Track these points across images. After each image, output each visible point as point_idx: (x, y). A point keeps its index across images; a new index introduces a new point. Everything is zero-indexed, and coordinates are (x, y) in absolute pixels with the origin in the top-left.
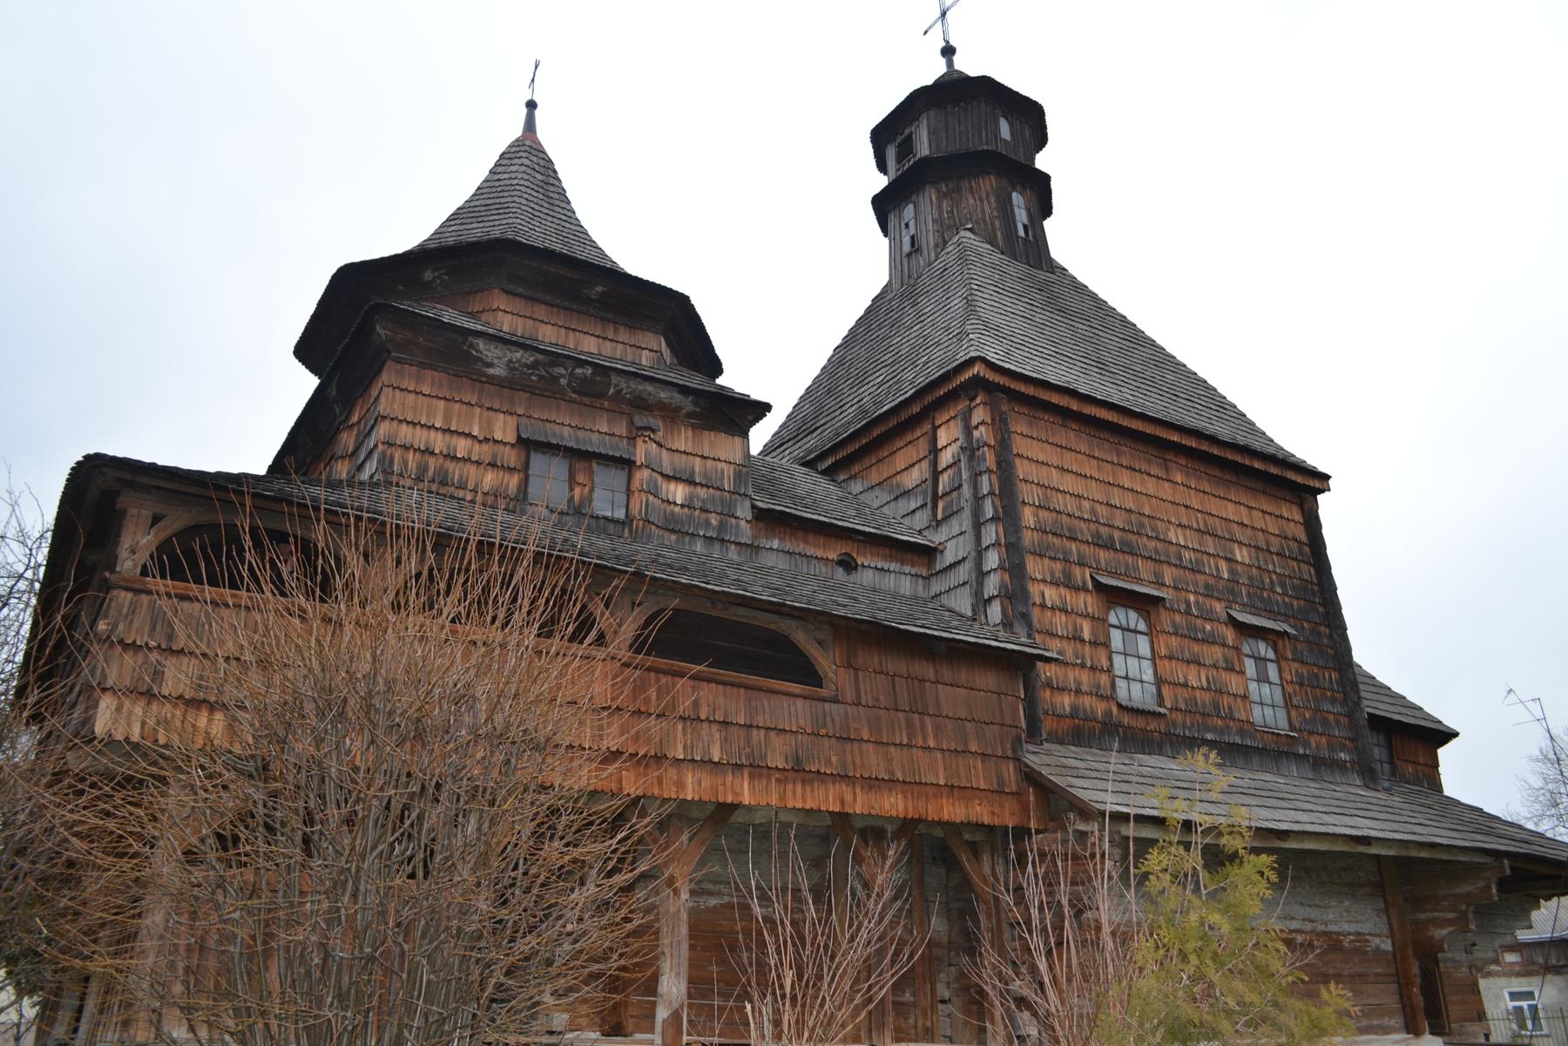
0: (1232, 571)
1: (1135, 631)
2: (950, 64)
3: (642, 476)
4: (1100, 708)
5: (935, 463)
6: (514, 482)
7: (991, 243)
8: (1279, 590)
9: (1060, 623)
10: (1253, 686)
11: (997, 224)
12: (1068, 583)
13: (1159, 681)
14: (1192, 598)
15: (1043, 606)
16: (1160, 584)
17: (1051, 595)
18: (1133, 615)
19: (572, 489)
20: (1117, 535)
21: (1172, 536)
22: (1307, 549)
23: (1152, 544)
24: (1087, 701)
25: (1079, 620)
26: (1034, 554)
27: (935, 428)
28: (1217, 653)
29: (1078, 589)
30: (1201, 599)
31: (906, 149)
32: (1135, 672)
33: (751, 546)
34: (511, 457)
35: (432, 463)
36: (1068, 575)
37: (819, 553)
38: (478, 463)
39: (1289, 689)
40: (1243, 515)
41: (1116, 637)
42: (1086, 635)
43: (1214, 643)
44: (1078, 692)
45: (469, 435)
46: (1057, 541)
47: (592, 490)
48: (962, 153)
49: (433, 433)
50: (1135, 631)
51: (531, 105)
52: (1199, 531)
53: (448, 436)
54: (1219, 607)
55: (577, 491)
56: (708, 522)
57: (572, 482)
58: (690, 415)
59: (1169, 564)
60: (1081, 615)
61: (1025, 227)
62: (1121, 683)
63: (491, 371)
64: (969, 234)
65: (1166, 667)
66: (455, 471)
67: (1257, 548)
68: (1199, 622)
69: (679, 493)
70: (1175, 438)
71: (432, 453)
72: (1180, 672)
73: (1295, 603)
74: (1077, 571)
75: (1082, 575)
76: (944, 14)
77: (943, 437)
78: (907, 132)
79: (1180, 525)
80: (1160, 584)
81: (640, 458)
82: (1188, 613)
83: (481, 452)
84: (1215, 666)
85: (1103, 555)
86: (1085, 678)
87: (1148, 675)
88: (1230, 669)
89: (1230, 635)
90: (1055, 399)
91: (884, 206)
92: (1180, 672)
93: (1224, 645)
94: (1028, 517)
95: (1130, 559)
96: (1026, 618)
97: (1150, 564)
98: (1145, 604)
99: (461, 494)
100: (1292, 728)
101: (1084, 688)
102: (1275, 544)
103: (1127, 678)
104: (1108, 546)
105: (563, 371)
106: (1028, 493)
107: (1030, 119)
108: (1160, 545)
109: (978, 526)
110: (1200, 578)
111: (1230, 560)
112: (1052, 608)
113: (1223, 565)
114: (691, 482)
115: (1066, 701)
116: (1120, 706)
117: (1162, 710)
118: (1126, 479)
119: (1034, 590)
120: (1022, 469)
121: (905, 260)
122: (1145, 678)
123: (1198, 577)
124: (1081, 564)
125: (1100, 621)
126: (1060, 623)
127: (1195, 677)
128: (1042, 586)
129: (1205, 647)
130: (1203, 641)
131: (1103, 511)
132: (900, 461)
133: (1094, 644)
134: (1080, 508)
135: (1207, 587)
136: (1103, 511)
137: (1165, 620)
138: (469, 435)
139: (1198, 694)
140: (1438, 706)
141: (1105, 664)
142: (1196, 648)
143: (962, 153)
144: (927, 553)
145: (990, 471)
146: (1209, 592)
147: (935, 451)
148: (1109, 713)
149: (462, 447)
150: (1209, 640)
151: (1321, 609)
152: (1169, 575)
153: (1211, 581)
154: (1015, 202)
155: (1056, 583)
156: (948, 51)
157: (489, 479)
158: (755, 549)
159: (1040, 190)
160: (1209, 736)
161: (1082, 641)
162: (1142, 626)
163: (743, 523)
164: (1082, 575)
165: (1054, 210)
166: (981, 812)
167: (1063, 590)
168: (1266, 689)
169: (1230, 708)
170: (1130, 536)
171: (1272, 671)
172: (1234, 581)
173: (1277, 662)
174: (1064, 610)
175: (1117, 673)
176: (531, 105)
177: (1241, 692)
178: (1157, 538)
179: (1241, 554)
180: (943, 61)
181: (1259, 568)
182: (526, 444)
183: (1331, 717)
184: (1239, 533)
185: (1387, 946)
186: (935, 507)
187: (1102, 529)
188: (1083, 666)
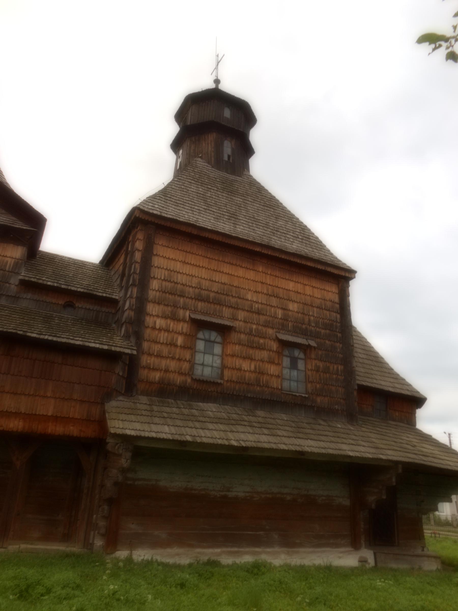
1: (214, 342)
4: (179, 379)
7: (208, 163)
10: (286, 372)
11: (213, 154)
12: (174, 318)
13: (223, 367)
14: (254, 327)
15: (154, 328)
17: (160, 323)
20: (212, 295)
21: (249, 297)
22: (338, 306)
23: (233, 300)
24: (171, 376)
25: (176, 336)
26: (154, 302)
28: (265, 354)
29: (179, 320)
30: (260, 328)
32: (208, 361)
33: (15, 297)
37: (54, 301)
39: (309, 373)
40: (299, 288)
41: (200, 345)
43: (263, 349)
50: (214, 342)
52: (267, 294)
54: (270, 331)
59: (243, 310)
60: (179, 333)
61: (229, 157)
62: (196, 367)
64: (199, 159)
65: (230, 361)
68: (256, 339)
70: (258, 249)
72: (238, 362)
73: (323, 331)
80: (234, 319)
85: (200, 305)
86: (173, 365)
88: (271, 362)
90: (183, 228)
92: (238, 362)
93: (270, 350)
94: (155, 284)
95: (218, 307)
97: (231, 310)
98: (224, 330)
102: (318, 302)
103: (203, 365)
104: (206, 300)
106: (155, 272)
108: (239, 301)
110: (262, 318)
112: (160, 330)
115: (157, 376)
117: (222, 382)
118: (226, 268)
119: (149, 321)
120: (156, 261)
122: (215, 365)
123: (261, 317)
124: (185, 308)
126: (163, 337)
127: (246, 365)
128: (155, 318)
129: (257, 352)
130: (257, 348)
133: (184, 347)
137: (234, 336)
139: (247, 374)
140: (419, 383)
141: (188, 357)
142: (251, 351)
144: (113, 302)
145: (137, 262)
146: (266, 325)
150: (261, 348)
151: (339, 335)
152: (241, 315)
155: (165, 317)
158: (16, 298)
160: (249, 396)
161: (176, 346)
162: (219, 339)
163: (13, 286)
165: (255, 150)
166: (73, 430)
167: (169, 321)
168: (295, 373)
170: (221, 296)
172: (285, 318)
173: (305, 360)
174: (167, 330)
175: (197, 362)
179: (293, 307)
184: (293, 296)
185: (347, 502)
188: (173, 358)
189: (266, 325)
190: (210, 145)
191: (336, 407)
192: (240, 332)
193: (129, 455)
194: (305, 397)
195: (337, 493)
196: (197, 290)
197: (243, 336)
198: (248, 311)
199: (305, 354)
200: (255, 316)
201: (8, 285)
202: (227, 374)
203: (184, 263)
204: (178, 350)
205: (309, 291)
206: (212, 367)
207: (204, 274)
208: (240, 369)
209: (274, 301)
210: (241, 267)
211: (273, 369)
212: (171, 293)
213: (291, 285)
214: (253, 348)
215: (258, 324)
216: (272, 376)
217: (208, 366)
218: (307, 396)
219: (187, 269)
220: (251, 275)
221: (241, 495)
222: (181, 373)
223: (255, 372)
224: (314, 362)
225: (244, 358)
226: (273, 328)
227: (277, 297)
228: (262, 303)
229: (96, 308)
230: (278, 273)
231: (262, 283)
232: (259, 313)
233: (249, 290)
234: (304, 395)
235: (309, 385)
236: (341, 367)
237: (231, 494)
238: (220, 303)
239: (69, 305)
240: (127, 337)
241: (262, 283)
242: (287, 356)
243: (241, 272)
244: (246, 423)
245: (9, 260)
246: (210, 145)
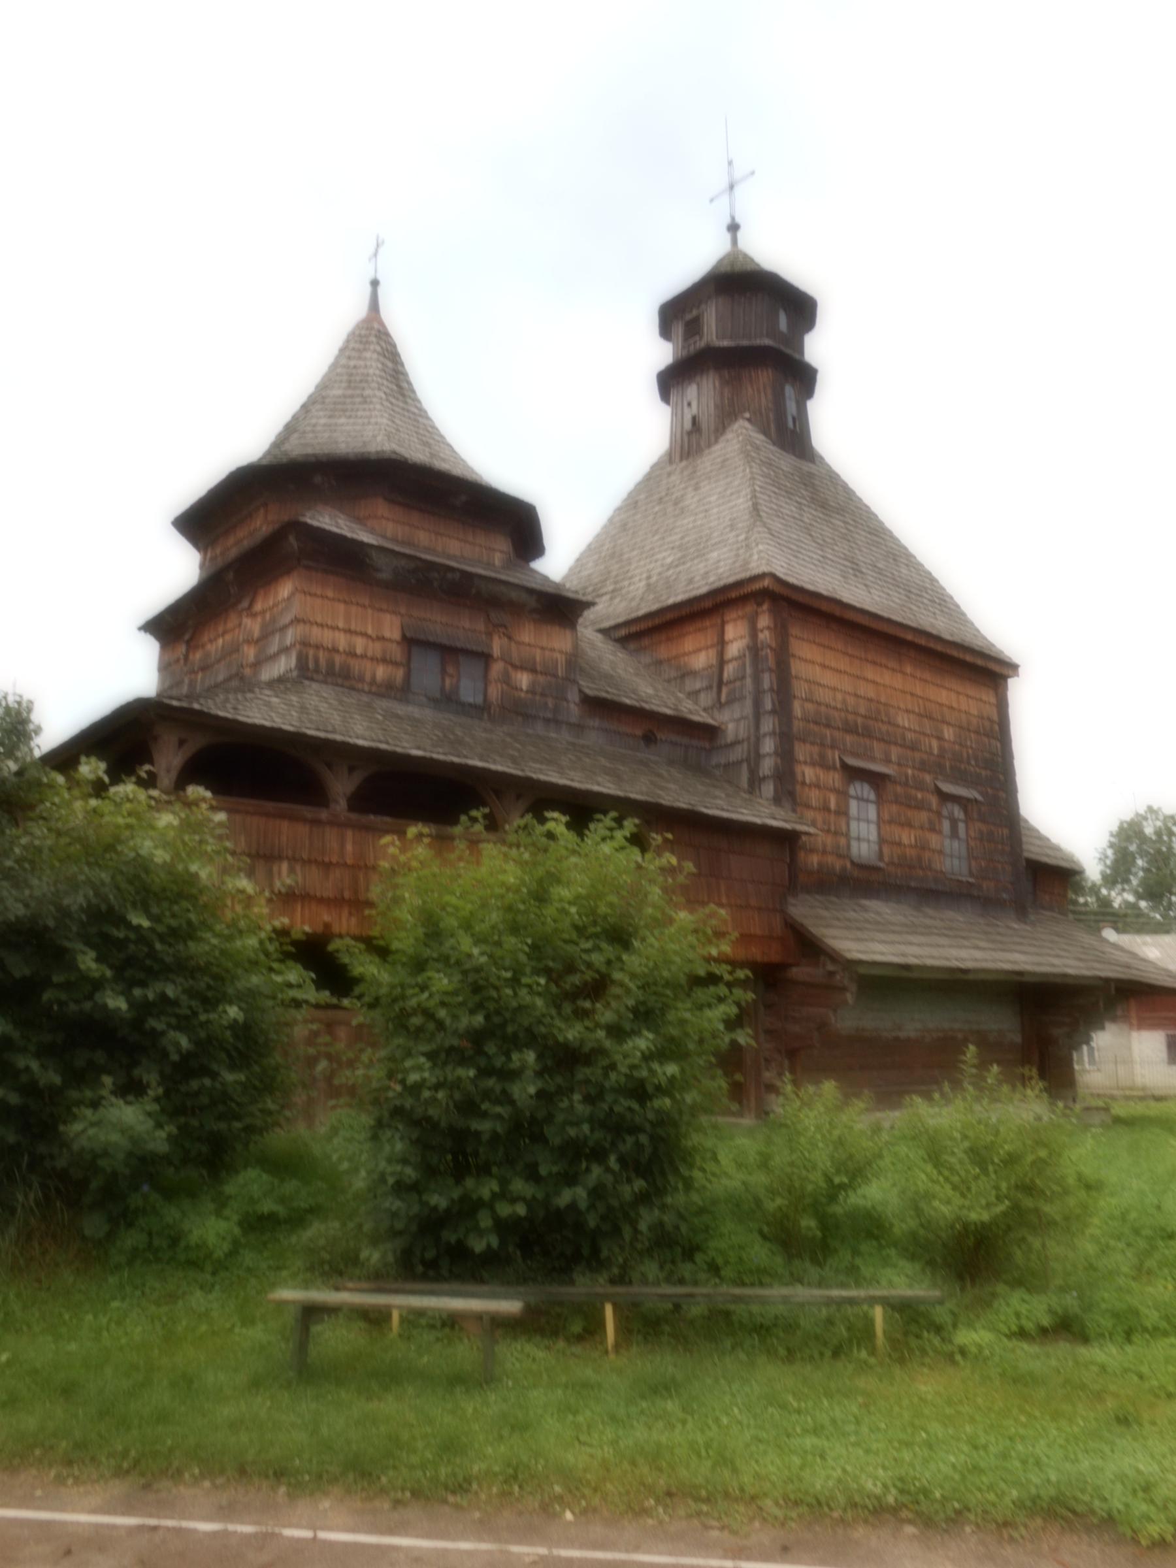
0: (941, 748)
2: (734, 241)
3: (497, 668)
4: (838, 864)
5: (721, 654)
6: (400, 674)
8: (973, 762)
9: (814, 796)
10: (947, 842)
11: (771, 416)
12: (822, 763)
13: (882, 841)
14: (910, 772)
15: (803, 783)
16: (888, 761)
18: (866, 787)
20: (860, 720)
21: (903, 720)
23: (884, 728)
24: (830, 859)
28: (924, 816)
30: (916, 772)
31: (693, 328)
32: (864, 831)
34: (397, 652)
35: (338, 659)
36: (822, 756)
38: (372, 659)
39: (972, 843)
41: (853, 805)
42: (833, 806)
44: (824, 852)
45: (364, 635)
46: (816, 728)
47: (458, 681)
48: (741, 341)
49: (337, 634)
50: (867, 801)
51: (375, 284)
52: (920, 715)
53: (348, 636)
54: (928, 778)
55: (448, 681)
56: (546, 704)
57: (444, 672)
62: (854, 844)
66: (356, 665)
67: (961, 727)
68: (913, 792)
69: (524, 680)
70: (909, 637)
71: (337, 651)
73: (983, 773)
74: (829, 753)
75: (834, 756)
76: (731, 187)
77: (731, 631)
78: (695, 312)
79: (907, 711)
81: (496, 651)
82: (906, 784)
83: (376, 649)
84: (922, 828)
85: (849, 739)
87: (873, 836)
88: (932, 829)
89: (934, 801)
90: (824, 607)
91: (670, 381)
93: (930, 810)
94: (797, 709)
96: (792, 795)
98: (876, 780)
100: (971, 874)
101: (829, 849)
105: (436, 575)
106: (800, 689)
107: (799, 308)
109: (757, 716)
110: (917, 755)
111: (940, 738)
114: (533, 670)
116: (852, 863)
117: (882, 865)
118: (870, 673)
120: (797, 667)
121: (689, 444)
125: (843, 795)
131: (851, 701)
132: (689, 643)
134: (834, 699)
136: (851, 701)
138: (364, 635)
142: (910, 813)
143: (741, 341)
144: (709, 732)
146: (923, 767)
147: (722, 643)
148: (844, 869)
149: (360, 644)
150: (920, 806)
152: (895, 753)
153: (925, 757)
154: (787, 394)
156: (734, 228)
157: (381, 672)
159: (803, 378)
160: (913, 884)
162: (872, 796)
163: (572, 706)
164: (834, 756)
168: (956, 844)
169: (929, 860)
171: (961, 826)
172: (941, 755)
173: (966, 822)
174: (818, 786)
176: (375, 284)
177: (938, 848)
178: (889, 723)
179: (948, 733)
180: (728, 237)
181: (961, 745)
182: (412, 642)
183: (1000, 866)
185: (1017, 1038)
189: (923, 767)
190: (762, 394)
191: (1005, 896)
192: (895, 782)
193: (854, 988)
194: (968, 882)
195: (1003, 1023)
196: (843, 714)
197: (899, 789)
198: (901, 746)
199: (966, 812)
200: (909, 753)
201: (565, 704)
202: (886, 850)
203: (824, 666)
204: (832, 818)
205: (964, 704)
206: (869, 841)
207: (846, 684)
208: (899, 844)
209: (928, 726)
210: (887, 667)
211: (934, 840)
212: (816, 723)
213: (944, 696)
214: (909, 806)
215: (914, 767)
216: (934, 851)
217: (864, 840)
218: (971, 880)
219: (829, 679)
220: (897, 681)
221: (913, 1035)
222: (840, 856)
223: (916, 846)
224: (978, 825)
225: (902, 825)
226: (929, 772)
227: (931, 718)
228: (915, 731)
229: (685, 740)
230: (927, 676)
231: (912, 694)
232: (914, 747)
233: (899, 708)
234: (964, 879)
235: (973, 863)
236: (1006, 831)
237: (902, 1035)
238: (868, 733)
239: (649, 739)
240: (777, 800)
241: (912, 694)
242: (946, 818)
243: (886, 678)
244: (897, 928)
245: (558, 655)
246: (762, 394)
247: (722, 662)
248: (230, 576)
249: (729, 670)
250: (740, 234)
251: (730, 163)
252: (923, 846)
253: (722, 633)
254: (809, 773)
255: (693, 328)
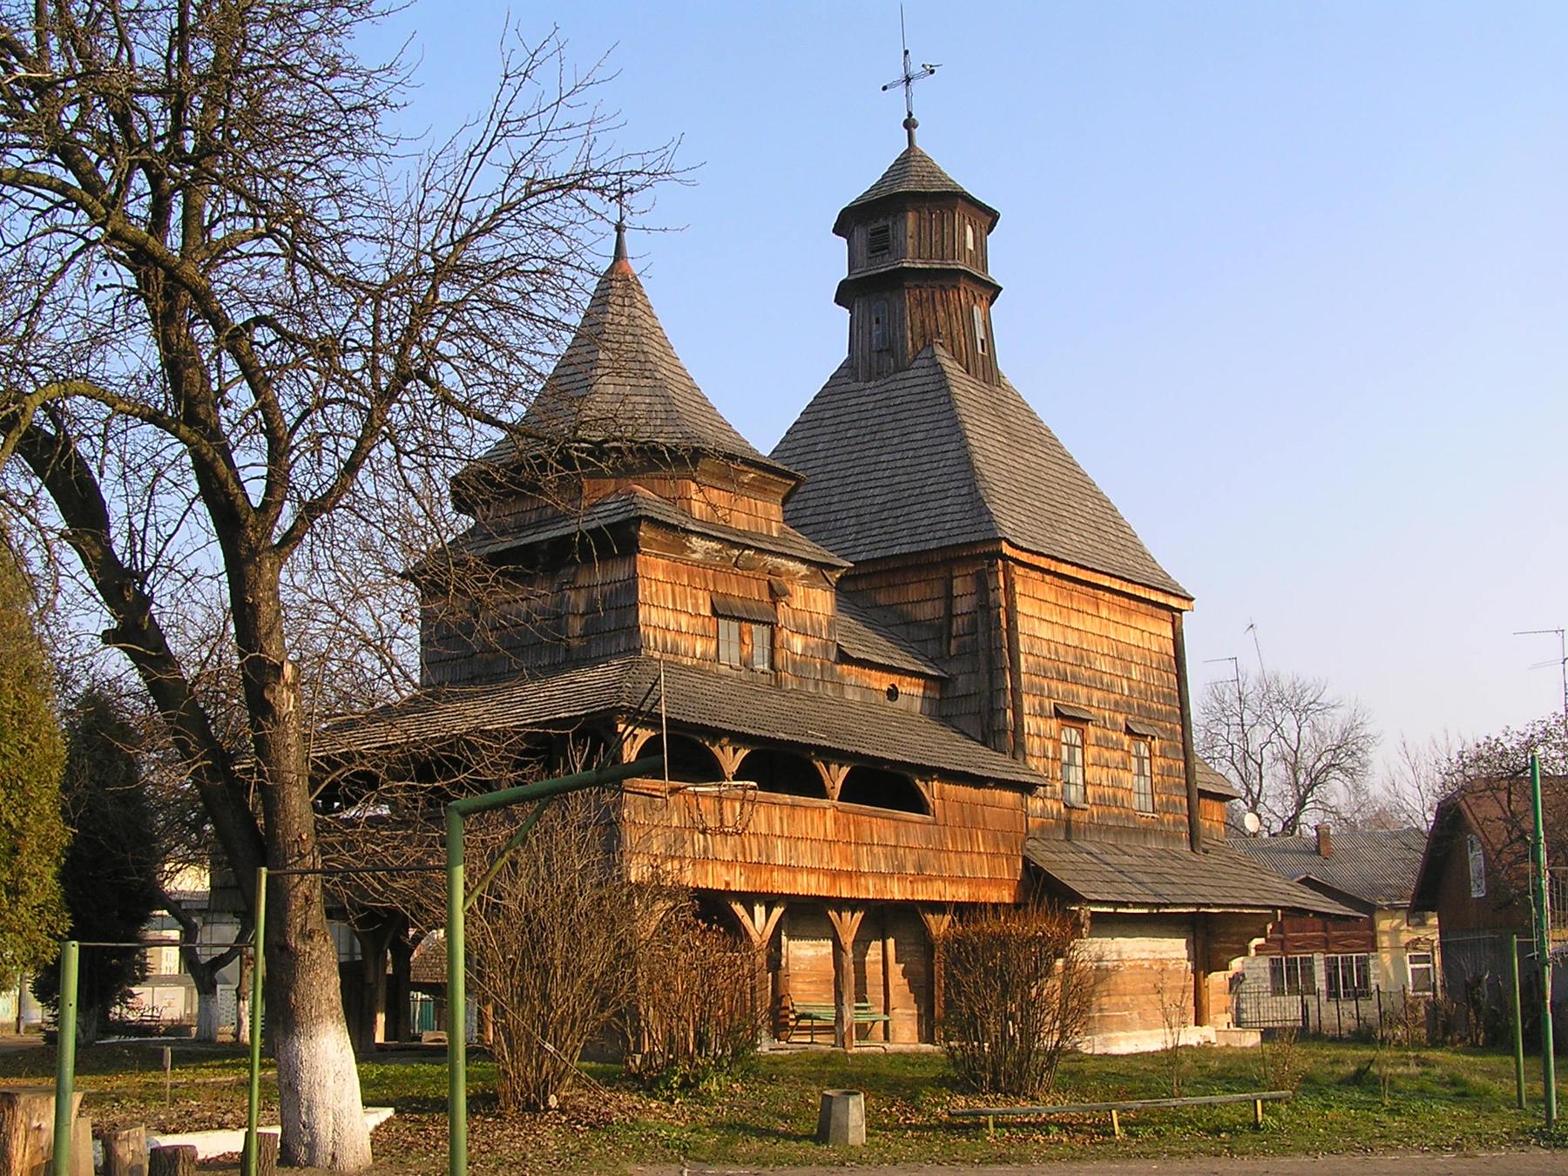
5: (949, 608)
19: (741, 649)
23: (1087, 674)
27: (952, 578)
28: (1118, 755)
31: (880, 244)
36: (1041, 705)
42: (1050, 755)
58: (803, 578)
63: (695, 556)
66: (684, 643)
75: (1049, 705)
77: (959, 586)
78: (882, 223)
99: (687, 661)
110: (1112, 696)
113: (1125, 682)
127: (1103, 775)
132: (913, 593)
135: (1117, 703)
147: (949, 598)
150: (1118, 746)
156: (909, 124)
186: (949, 644)
187: (1061, 666)
247: (950, 615)
248: (545, 547)
249: (958, 625)
250: (915, 131)
251: (906, 52)
252: (1116, 784)
253: (949, 588)
254: (1030, 723)
255: (880, 244)
